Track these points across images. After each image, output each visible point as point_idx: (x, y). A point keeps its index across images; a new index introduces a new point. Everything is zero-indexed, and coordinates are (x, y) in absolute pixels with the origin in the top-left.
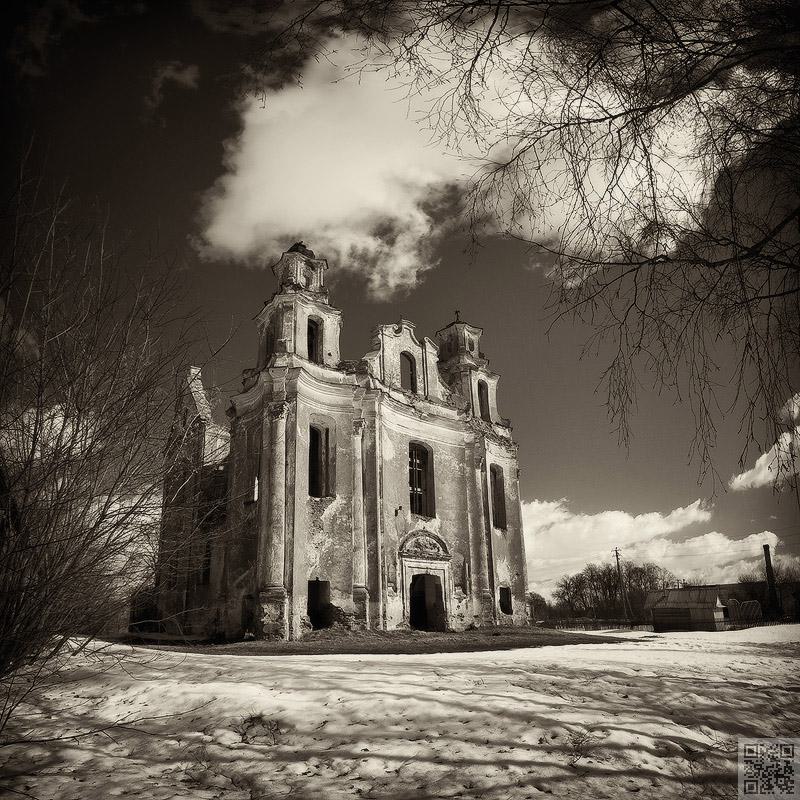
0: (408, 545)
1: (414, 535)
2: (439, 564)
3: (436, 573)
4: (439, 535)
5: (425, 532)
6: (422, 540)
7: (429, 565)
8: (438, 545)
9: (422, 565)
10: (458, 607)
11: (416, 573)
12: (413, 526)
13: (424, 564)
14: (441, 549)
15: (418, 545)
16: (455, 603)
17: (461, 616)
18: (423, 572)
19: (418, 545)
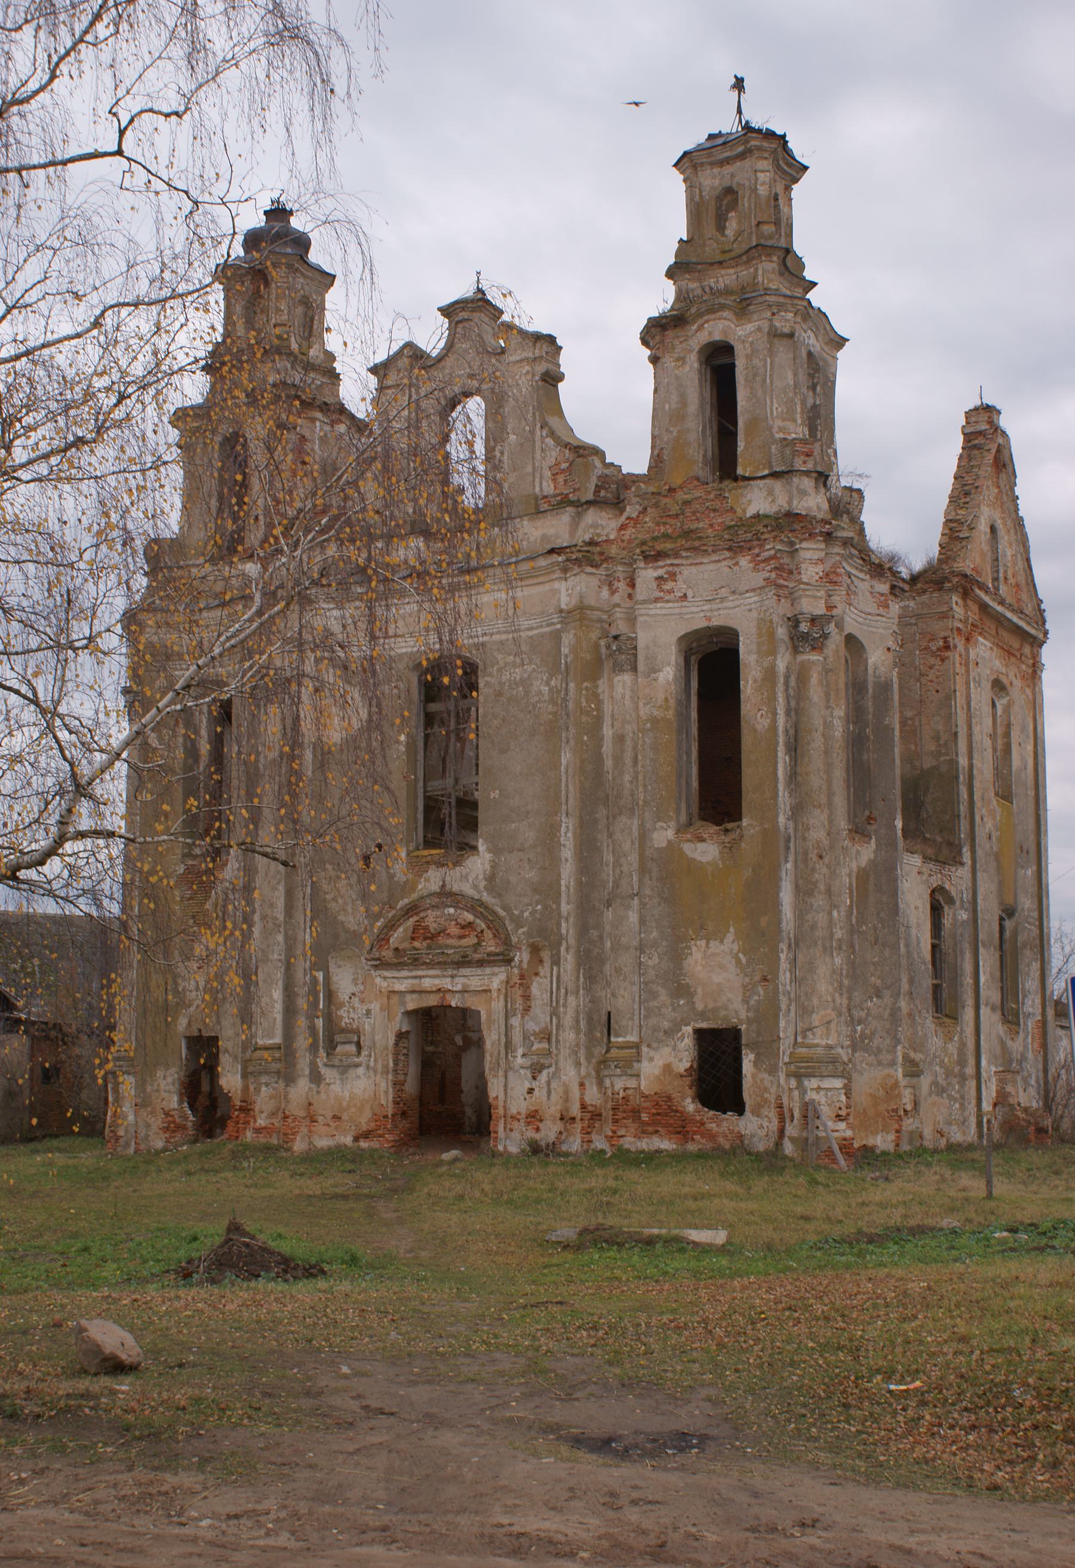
0: (397, 937)
1: (412, 909)
2: (473, 978)
3: (472, 1002)
4: (486, 897)
5: (446, 896)
6: (432, 919)
7: (446, 983)
8: (481, 924)
9: (427, 983)
10: (531, 1091)
11: (411, 1006)
12: (408, 887)
13: (431, 980)
14: (488, 934)
15: (419, 932)
16: (520, 1083)
17: (534, 1117)
18: (432, 1001)
19: (419, 932)
